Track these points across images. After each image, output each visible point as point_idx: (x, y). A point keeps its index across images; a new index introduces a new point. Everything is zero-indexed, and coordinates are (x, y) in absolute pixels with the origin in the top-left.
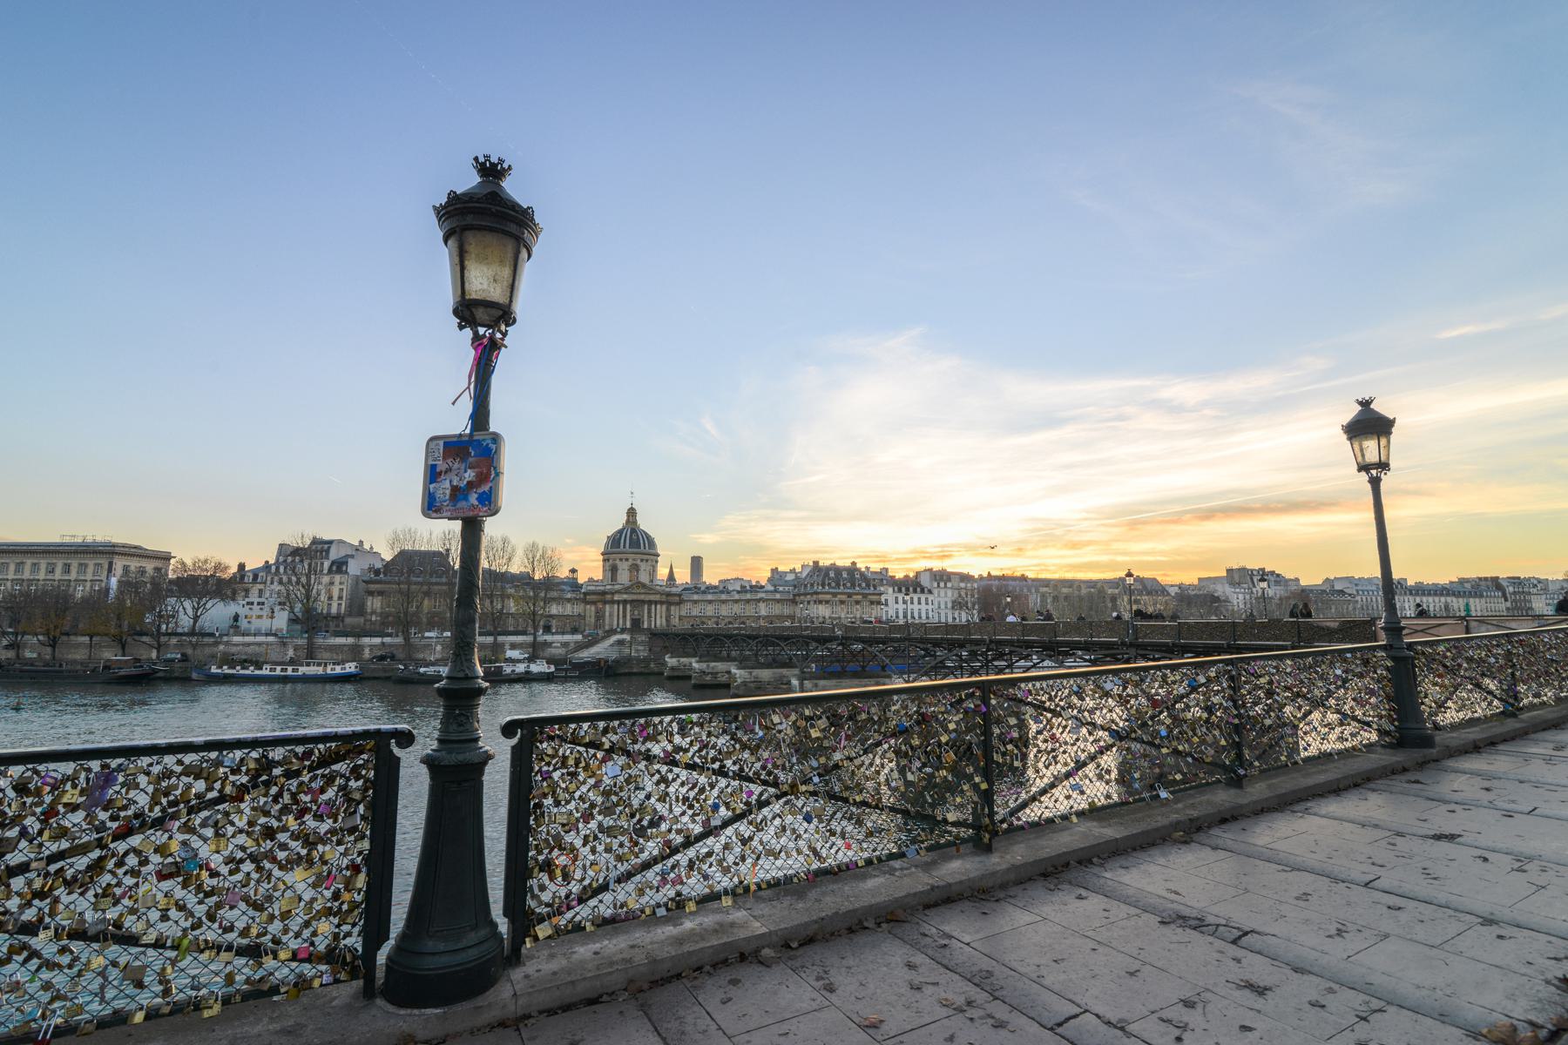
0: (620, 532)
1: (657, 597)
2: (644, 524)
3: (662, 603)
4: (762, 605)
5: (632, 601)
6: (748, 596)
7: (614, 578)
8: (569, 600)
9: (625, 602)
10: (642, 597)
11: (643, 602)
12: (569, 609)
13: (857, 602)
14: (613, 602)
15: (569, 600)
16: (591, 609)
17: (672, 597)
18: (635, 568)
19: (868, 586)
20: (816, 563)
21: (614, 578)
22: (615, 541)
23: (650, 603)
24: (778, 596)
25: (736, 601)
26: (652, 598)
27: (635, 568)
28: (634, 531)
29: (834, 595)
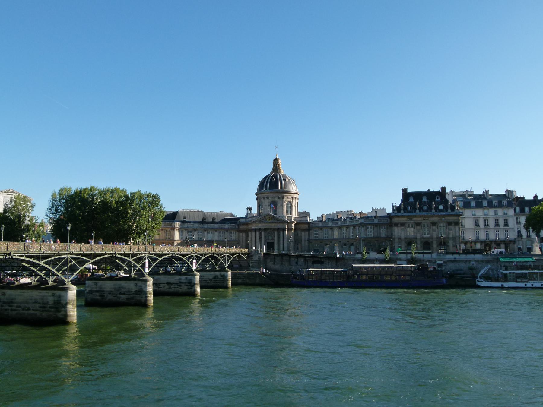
5: (265, 230)
9: (260, 230)
10: (273, 226)
13: (434, 224)
15: (227, 230)
19: (446, 208)
20: (404, 191)
24: (376, 221)
26: (280, 226)
29: (410, 218)
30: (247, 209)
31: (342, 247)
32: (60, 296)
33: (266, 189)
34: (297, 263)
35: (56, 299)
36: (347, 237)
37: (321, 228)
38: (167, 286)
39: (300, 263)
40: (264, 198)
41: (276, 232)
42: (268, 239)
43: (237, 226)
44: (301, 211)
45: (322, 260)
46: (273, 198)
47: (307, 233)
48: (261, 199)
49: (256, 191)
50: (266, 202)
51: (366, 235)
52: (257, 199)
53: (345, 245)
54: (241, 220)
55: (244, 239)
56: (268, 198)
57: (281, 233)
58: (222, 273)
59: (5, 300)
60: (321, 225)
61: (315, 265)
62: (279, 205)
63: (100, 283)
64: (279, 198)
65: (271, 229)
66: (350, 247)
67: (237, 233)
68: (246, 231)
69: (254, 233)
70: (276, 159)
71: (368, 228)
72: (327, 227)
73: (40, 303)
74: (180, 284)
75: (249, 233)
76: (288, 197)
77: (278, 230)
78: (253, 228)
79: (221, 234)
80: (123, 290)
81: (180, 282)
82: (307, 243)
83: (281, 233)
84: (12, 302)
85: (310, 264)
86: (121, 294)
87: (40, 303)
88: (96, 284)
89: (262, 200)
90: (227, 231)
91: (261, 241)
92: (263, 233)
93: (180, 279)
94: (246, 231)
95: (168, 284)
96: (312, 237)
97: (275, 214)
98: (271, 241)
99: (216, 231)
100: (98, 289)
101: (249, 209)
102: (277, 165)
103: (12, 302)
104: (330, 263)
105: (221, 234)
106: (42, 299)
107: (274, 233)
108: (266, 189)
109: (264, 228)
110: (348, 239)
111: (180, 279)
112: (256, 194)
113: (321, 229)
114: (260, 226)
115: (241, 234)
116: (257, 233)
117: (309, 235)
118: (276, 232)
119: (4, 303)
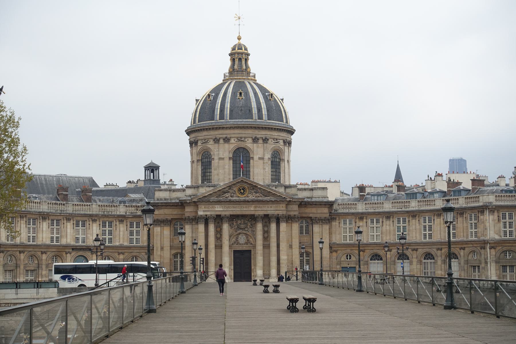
0: (217, 90)
1: (280, 210)
3: (289, 219)
4: (489, 219)
5: (232, 218)
6: (461, 202)
8: (122, 218)
9: (219, 219)
11: (253, 218)
12: (121, 235)
14: (195, 220)
15: (122, 218)
16: (163, 235)
17: (312, 210)
22: (207, 108)
23: (267, 219)
26: (271, 210)
27: (241, 158)
28: (240, 87)
30: (147, 168)
31: (421, 261)
33: (222, 117)
37: (361, 216)
40: (216, 141)
42: (237, 242)
46: (240, 139)
47: (326, 227)
48: (206, 141)
49: (188, 123)
51: (498, 234)
52: (191, 143)
53: (429, 256)
56: (227, 140)
57: (273, 226)
60: (361, 208)
62: (256, 157)
64: (255, 140)
65: (243, 216)
68: (176, 224)
69: (201, 227)
70: (240, 46)
71: (504, 217)
72: (379, 213)
75: (188, 229)
76: (276, 140)
79: (107, 228)
82: (326, 252)
83: (273, 226)
89: (211, 145)
90: (121, 221)
94: (176, 224)
96: (338, 239)
98: (245, 248)
99: (94, 221)
102: (240, 59)
105: (107, 228)
107: (253, 226)
108: (222, 117)
109: (228, 213)
112: (189, 132)
113: (361, 219)
114: (218, 209)
115: (157, 230)
116: (212, 228)
117: (330, 233)
118: (259, 226)
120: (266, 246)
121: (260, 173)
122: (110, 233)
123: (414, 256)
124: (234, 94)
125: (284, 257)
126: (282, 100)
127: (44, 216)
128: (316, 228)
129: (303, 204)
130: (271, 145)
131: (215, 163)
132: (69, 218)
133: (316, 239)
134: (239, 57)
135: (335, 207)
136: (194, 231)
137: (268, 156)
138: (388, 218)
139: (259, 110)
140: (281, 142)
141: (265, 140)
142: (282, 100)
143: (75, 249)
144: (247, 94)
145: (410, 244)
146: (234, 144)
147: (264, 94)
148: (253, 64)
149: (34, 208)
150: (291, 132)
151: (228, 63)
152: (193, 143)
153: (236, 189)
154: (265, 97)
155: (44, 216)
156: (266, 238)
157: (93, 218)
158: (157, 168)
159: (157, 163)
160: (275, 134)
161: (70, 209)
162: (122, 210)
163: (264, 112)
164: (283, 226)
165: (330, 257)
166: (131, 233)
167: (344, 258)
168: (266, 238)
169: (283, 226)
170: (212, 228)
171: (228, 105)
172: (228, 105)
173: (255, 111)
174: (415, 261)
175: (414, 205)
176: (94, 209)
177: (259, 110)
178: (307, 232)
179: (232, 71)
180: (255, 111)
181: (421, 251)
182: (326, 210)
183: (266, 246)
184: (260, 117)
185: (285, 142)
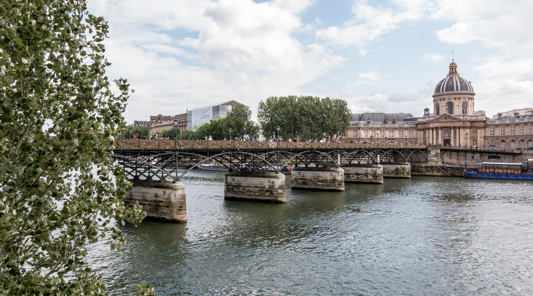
1: (461, 124)
2: (463, 72)
3: (464, 128)
5: (442, 128)
7: (438, 114)
8: (406, 129)
9: (437, 128)
10: (449, 125)
12: (406, 134)
14: (429, 129)
15: (406, 129)
18: (450, 106)
21: (438, 114)
25: (526, 124)
26: (456, 124)
28: (451, 79)
30: (425, 110)
32: (273, 183)
33: (443, 91)
34: (472, 157)
35: (271, 184)
36: (525, 134)
37: (497, 126)
38: (356, 176)
39: (475, 158)
40: (441, 100)
41: (452, 131)
43: (415, 126)
44: (476, 109)
45: (499, 155)
46: (449, 99)
47: (483, 130)
48: (437, 100)
50: (443, 105)
53: (522, 141)
54: (419, 120)
55: (422, 137)
56: (444, 99)
57: (458, 130)
58: (403, 166)
59: (235, 185)
61: (491, 159)
62: (455, 105)
63: (302, 173)
64: (455, 99)
66: (528, 143)
67: (416, 131)
68: (424, 130)
69: (431, 131)
73: (258, 187)
74: (366, 175)
75: (427, 131)
77: (454, 128)
78: (430, 126)
80: (320, 179)
81: (367, 173)
82: (483, 139)
83: (458, 130)
84: (240, 186)
85: (486, 158)
86: (318, 181)
87: (258, 187)
88: (300, 173)
89: (439, 101)
91: (437, 138)
92: (440, 131)
93: (367, 170)
95: (357, 174)
96: (488, 134)
97: (452, 113)
100: (301, 177)
101: (427, 110)
103: (240, 186)
104: (507, 158)
106: (261, 184)
107: (450, 130)
110: (526, 135)
111: (367, 170)
112: (433, 97)
113: (497, 127)
114: (437, 125)
115: (419, 132)
116: (435, 132)
117: (485, 132)
118: (452, 131)
119: (235, 186)
120: (455, 138)
121: (457, 111)
122: (402, 134)
123: (517, 141)
124: (448, 82)
125: (461, 142)
126: (470, 82)
127: (378, 129)
128: (479, 131)
129: (471, 122)
130: (462, 100)
131: (440, 108)
132: (387, 129)
133: (479, 135)
134: (453, 68)
135: (487, 122)
136: (429, 133)
137: (461, 104)
138: (508, 126)
139: (457, 87)
140: (467, 99)
141: (459, 99)
142: (470, 82)
143: (389, 139)
144: (453, 82)
145: (515, 136)
146: (447, 101)
147: (460, 81)
148: (458, 70)
149: (375, 126)
150: (474, 95)
151: (449, 70)
152: (434, 101)
153: (443, 117)
154: (461, 83)
155: (378, 129)
156: (455, 135)
157: (396, 129)
158: (429, 110)
159: (428, 108)
160: (464, 96)
161: (387, 126)
162: (406, 126)
163: (459, 88)
164: (461, 130)
165: (484, 142)
166: (410, 134)
167: (490, 142)
168: (455, 135)
169: (461, 130)
170: (435, 132)
171: (445, 87)
172: (445, 87)
173: (455, 88)
174: (517, 142)
175: (517, 121)
176: (396, 126)
177: (457, 87)
178: (476, 132)
179: (450, 73)
180: (455, 88)
181: (519, 139)
182: (483, 124)
183: (455, 138)
184: (457, 90)
185: (469, 99)
